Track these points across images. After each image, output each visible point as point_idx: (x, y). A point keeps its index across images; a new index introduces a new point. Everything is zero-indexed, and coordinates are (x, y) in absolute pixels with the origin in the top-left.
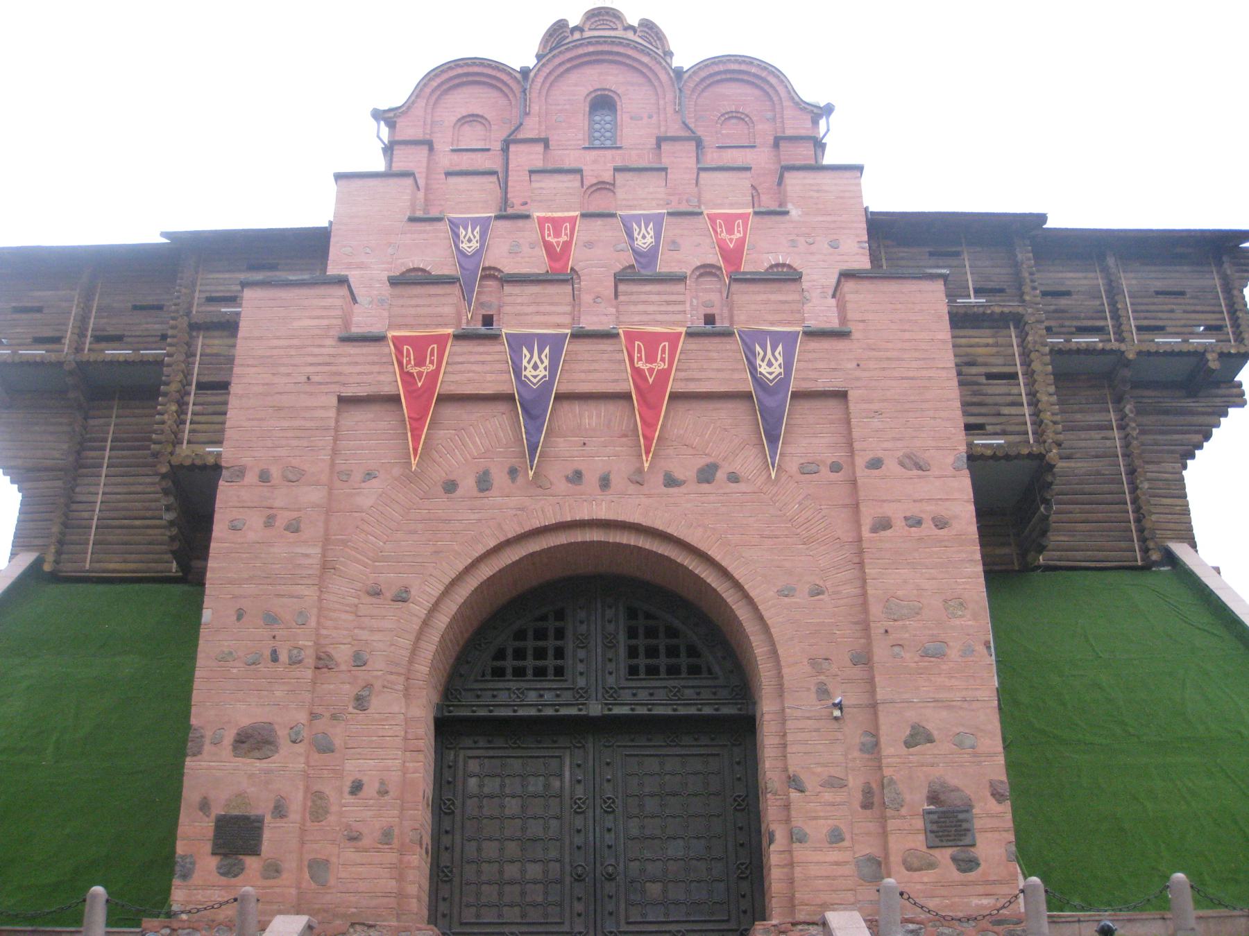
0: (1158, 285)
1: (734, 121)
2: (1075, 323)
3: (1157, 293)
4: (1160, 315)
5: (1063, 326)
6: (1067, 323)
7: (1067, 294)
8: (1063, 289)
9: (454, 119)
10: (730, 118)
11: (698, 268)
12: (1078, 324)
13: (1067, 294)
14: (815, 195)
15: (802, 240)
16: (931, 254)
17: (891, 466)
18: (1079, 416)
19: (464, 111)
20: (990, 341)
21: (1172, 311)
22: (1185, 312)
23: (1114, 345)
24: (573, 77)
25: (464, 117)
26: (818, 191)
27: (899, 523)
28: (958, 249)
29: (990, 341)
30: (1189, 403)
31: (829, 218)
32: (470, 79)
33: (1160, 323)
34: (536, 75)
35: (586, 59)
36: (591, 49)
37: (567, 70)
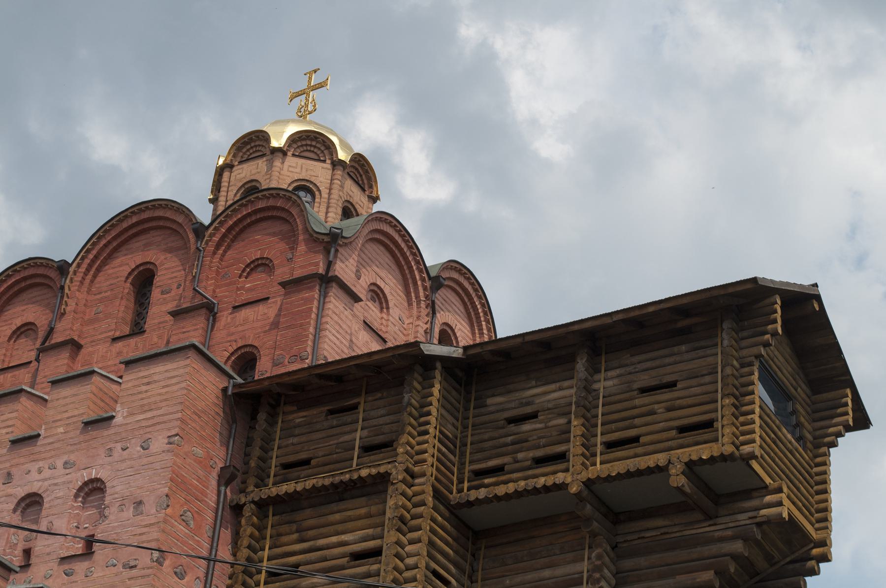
0: (645, 380)
2: (531, 454)
3: (644, 391)
4: (637, 421)
5: (516, 461)
6: (520, 456)
8: (528, 410)
9: (9, 332)
10: (259, 265)
11: (23, 499)
12: (539, 453)
13: (533, 416)
14: (144, 388)
15: (119, 446)
16: (331, 412)
18: (547, 573)
19: (18, 322)
20: (363, 511)
21: (652, 413)
22: (669, 410)
23: (560, 478)
25: (18, 328)
26: (148, 384)
28: (355, 401)
29: (363, 511)
30: (705, 529)
31: (149, 415)
33: (632, 433)
34: (79, 266)
36: (135, 219)
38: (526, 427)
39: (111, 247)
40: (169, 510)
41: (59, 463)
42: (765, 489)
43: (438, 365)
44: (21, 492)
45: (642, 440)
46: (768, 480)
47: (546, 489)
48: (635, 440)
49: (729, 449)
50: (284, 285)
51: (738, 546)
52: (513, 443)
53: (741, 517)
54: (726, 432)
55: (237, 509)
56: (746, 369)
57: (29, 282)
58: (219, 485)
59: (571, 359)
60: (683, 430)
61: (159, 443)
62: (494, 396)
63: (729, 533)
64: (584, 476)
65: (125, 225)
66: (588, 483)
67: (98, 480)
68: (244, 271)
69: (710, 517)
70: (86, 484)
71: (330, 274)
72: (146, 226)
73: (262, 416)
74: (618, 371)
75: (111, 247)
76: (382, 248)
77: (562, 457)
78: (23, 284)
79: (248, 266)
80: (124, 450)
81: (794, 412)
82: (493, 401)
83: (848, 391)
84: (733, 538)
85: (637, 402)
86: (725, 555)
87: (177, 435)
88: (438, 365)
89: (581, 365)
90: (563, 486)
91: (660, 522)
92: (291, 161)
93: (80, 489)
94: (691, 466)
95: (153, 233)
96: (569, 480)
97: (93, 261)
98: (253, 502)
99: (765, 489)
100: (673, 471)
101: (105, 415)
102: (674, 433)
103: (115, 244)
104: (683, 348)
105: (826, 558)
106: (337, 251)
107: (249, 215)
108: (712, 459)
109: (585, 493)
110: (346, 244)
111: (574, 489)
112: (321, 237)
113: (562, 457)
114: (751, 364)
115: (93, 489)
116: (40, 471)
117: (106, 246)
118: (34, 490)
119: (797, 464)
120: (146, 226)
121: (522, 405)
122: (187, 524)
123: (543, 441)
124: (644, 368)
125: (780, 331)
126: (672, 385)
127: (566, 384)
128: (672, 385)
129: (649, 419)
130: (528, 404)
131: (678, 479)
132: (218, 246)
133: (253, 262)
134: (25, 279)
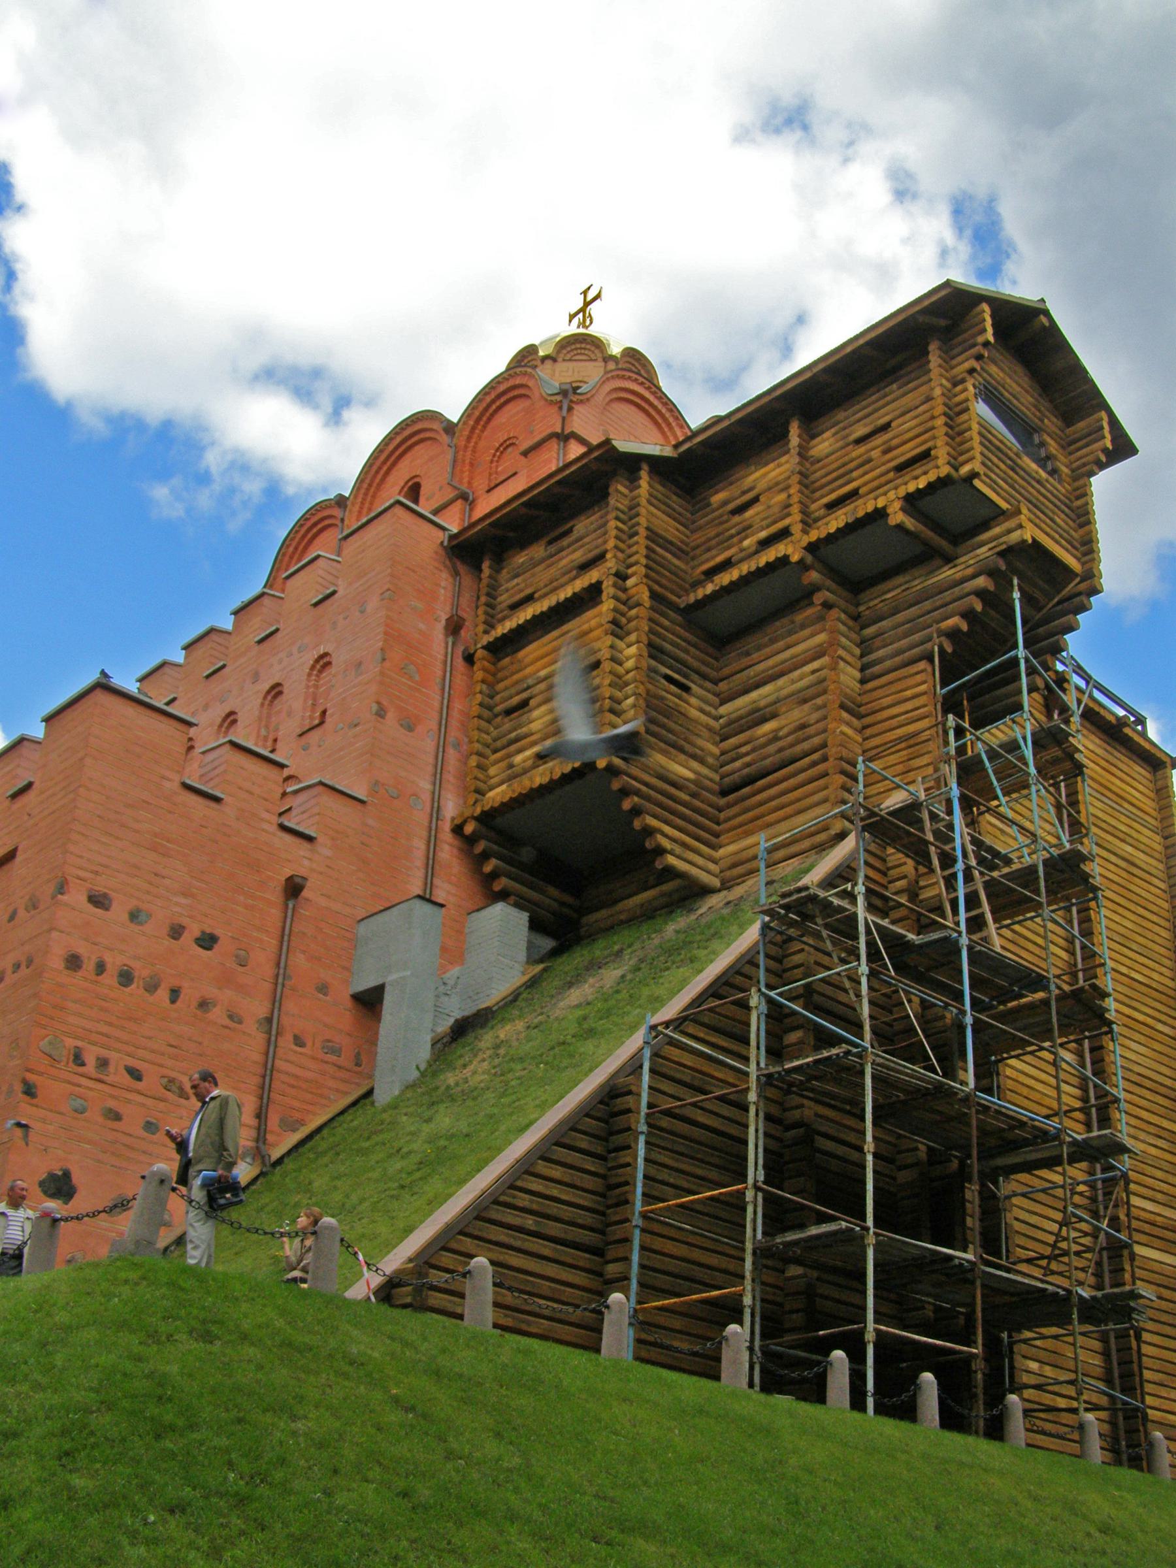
0: (860, 431)
1: (510, 450)
5: (742, 550)
6: (746, 543)
7: (756, 500)
11: (268, 692)
13: (756, 500)
15: (341, 617)
16: (550, 543)
17: (22, 913)
21: (870, 461)
22: (885, 452)
24: (391, 479)
27: (9, 971)
32: (315, 530)
35: (397, 453)
36: (399, 439)
37: (387, 473)
38: (749, 513)
39: (382, 472)
40: (387, 664)
41: (295, 650)
42: (999, 515)
43: (645, 467)
44: (267, 686)
45: (861, 491)
46: (1004, 505)
47: (770, 567)
48: (854, 494)
49: (945, 470)
50: (525, 454)
51: (982, 582)
52: (739, 533)
53: (979, 551)
54: (942, 453)
55: (469, 659)
56: (959, 388)
57: (320, 526)
58: (447, 636)
59: (784, 435)
60: (900, 468)
61: (373, 604)
62: (716, 493)
63: (970, 571)
64: (806, 540)
65: (391, 447)
66: (812, 548)
67: (326, 655)
68: (494, 455)
69: (949, 560)
70: (317, 661)
71: (566, 432)
72: (409, 443)
73: (486, 565)
74: (833, 430)
75: (382, 472)
76: (633, 408)
77: (785, 533)
78: (315, 530)
79: (497, 450)
80: (345, 618)
81: (1043, 444)
82: (717, 498)
83: (1103, 414)
84: (974, 576)
85: (854, 454)
86: (968, 594)
87: (388, 590)
88: (645, 467)
89: (794, 438)
90: (784, 561)
91: (900, 579)
92: (561, 366)
93: (313, 668)
94: (912, 501)
95: (417, 448)
96: (790, 551)
97: (368, 490)
98: (483, 647)
99: (999, 515)
100: (889, 511)
101: (328, 592)
102: (891, 474)
103: (385, 468)
104: (894, 386)
105: (1095, 591)
106: (570, 409)
107: (493, 401)
108: (931, 487)
109: (809, 559)
110: (581, 402)
111: (795, 558)
112: (553, 398)
113: (785, 533)
114: (963, 381)
115: (323, 662)
116: (280, 662)
117: (377, 472)
118: (276, 680)
119: (1048, 495)
120: (409, 443)
121: (744, 493)
122: (410, 678)
123: (764, 523)
124: (857, 420)
125: (991, 339)
126: (886, 427)
127: (783, 459)
128: (886, 427)
129: (867, 467)
130: (751, 489)
131: (897, 517)
132: (469, 439)
133: (501, 445)
134: (315, 524)
